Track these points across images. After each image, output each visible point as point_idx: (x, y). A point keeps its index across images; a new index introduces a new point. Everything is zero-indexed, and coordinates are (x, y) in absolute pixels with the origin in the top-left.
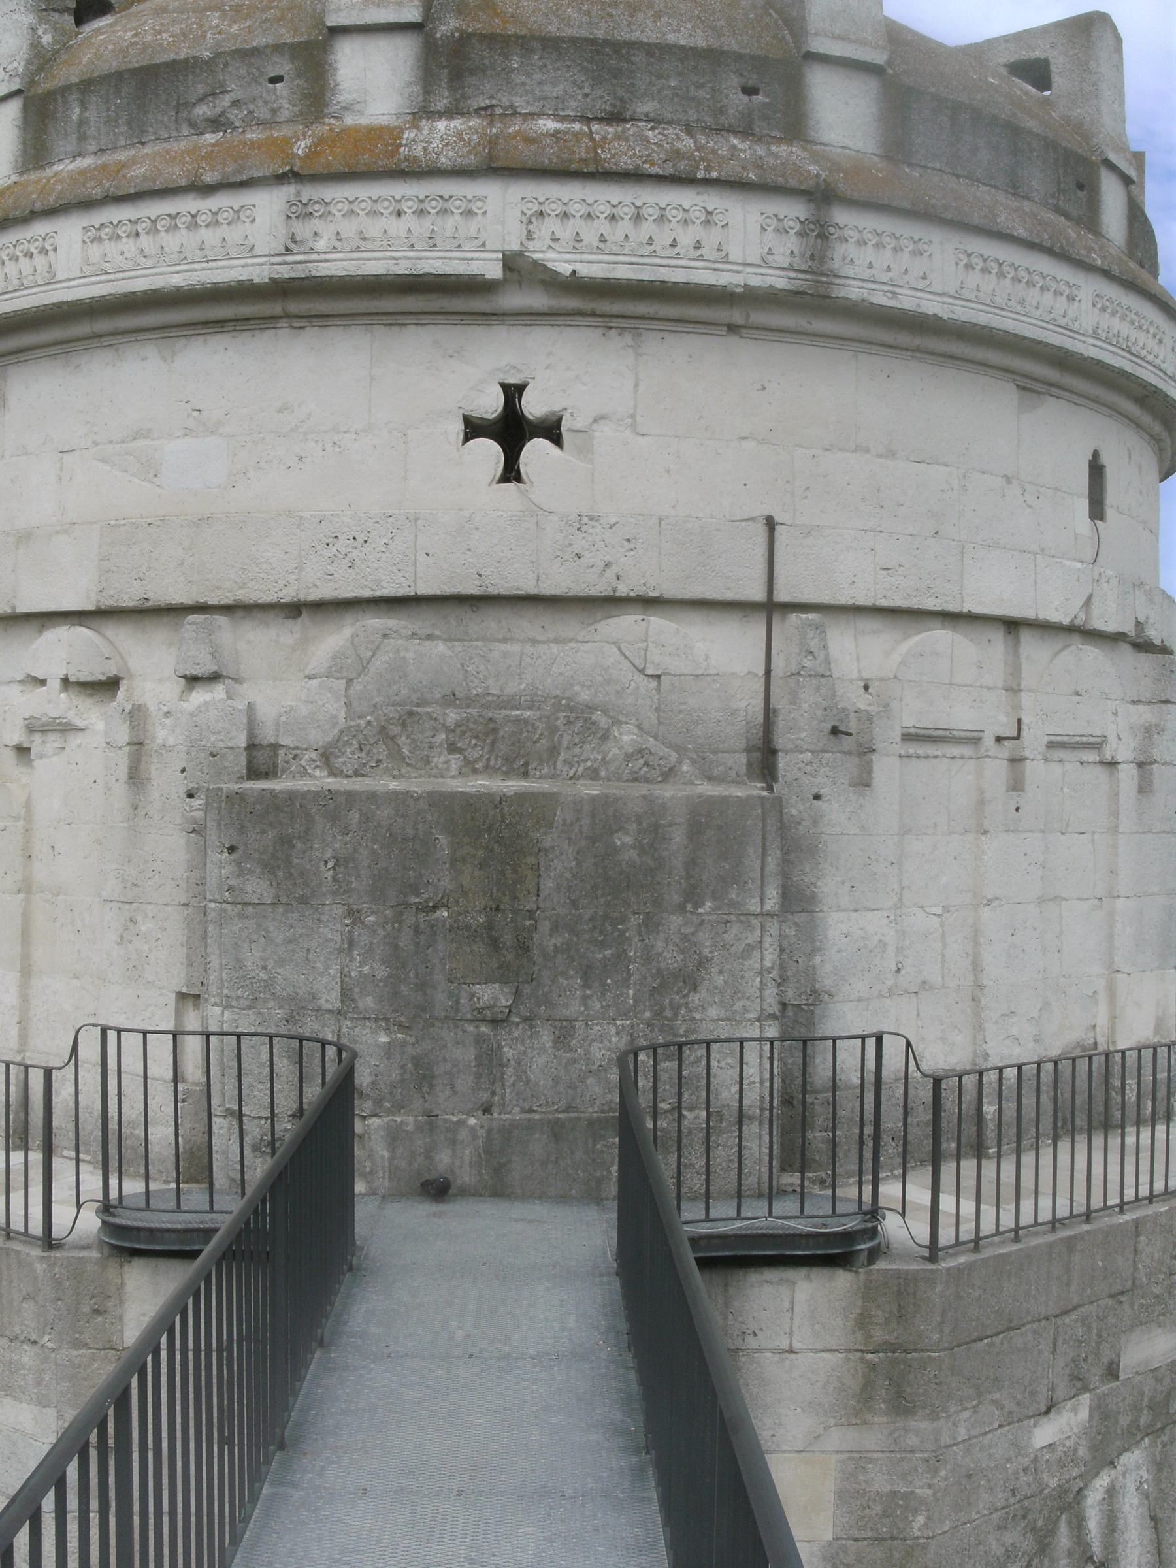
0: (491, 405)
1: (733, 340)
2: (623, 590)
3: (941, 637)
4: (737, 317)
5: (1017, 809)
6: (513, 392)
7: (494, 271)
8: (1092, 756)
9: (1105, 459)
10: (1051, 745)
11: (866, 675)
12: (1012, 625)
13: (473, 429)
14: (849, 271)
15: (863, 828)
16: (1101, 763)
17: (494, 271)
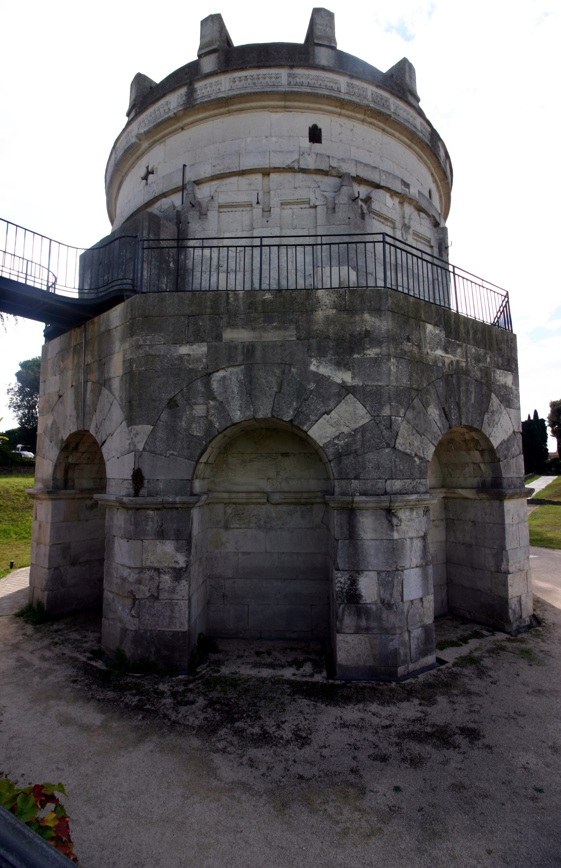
0: (143, 172)
1: (184, 132)
2: (156, 195)
3: (234, 179)
4: (180, 124)
5: (267, 221)
6: (147, 168)
7: (137, 141)
8: (307, 206)
9: (320, 126)
10: (282, 204)
11: (212, 195)
12: (266, 172)
13: (143, 179)
14: (198, 97)
15: (204, 229)
16: (311, 207)
17: (134, 140)
